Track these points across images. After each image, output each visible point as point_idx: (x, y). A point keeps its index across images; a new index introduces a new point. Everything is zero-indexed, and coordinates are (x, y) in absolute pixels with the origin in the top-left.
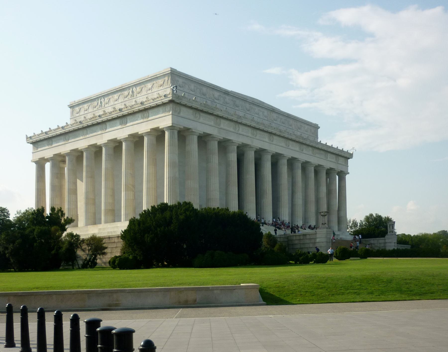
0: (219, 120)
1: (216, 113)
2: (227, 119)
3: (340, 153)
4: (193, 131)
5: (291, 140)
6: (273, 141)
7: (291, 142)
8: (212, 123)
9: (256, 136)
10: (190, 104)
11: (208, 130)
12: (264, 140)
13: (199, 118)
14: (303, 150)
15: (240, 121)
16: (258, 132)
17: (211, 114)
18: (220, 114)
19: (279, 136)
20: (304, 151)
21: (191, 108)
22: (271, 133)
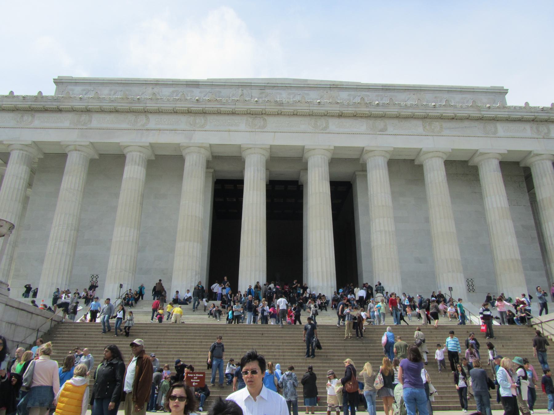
2: (102, 111)
3: (544, 116)
5: (326, 115)
12: (233, 128)
14: (384, 130)
16: (210, 118)
20: (390, 130)
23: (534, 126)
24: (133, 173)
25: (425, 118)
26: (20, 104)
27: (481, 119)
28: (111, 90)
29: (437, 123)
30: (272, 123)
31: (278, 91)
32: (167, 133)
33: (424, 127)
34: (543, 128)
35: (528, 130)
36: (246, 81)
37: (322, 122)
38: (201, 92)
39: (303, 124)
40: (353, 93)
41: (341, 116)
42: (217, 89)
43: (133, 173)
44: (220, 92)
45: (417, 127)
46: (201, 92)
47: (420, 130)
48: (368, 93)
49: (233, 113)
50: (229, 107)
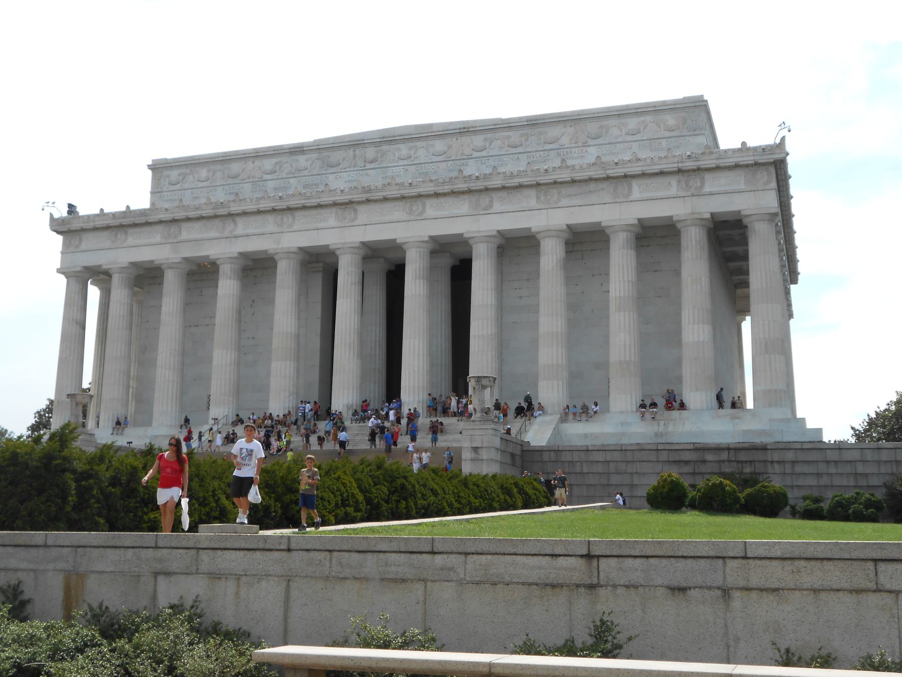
0: (174, 229)
1: (152, 219)
2: (188, 219)
4: (104, 267)
5: (420, 196)
6: (355, 219)
7: (429, 202)
8: (158, 238)
10: (91, 225)
11: (145, 255)
14: (490, 206)
15: (223, 211)
16: (298, 214)
17: (148, 224)
19: (368, 201)
20: (497, 206)
21: (95, 229)
22: (335, 204)
24: (227, 287)
25: (538, 185)
26: (111, 222)
27: (608, 178)
28: (209, 171)
29: (555, 191)
30: (364, 214)
31: (397, 146)
32: (257, 238)
34: (695, 182)
35: (673, 186)
36: (358, 138)
37: (417, 207)
39: (397, 212)
40: (489, 136)
41: (437, 195)
42: (326, 154)
43: (227, 287)
44: (329, 157)
45: (530, 199)
46: (307, 160)
49: (319, 206)
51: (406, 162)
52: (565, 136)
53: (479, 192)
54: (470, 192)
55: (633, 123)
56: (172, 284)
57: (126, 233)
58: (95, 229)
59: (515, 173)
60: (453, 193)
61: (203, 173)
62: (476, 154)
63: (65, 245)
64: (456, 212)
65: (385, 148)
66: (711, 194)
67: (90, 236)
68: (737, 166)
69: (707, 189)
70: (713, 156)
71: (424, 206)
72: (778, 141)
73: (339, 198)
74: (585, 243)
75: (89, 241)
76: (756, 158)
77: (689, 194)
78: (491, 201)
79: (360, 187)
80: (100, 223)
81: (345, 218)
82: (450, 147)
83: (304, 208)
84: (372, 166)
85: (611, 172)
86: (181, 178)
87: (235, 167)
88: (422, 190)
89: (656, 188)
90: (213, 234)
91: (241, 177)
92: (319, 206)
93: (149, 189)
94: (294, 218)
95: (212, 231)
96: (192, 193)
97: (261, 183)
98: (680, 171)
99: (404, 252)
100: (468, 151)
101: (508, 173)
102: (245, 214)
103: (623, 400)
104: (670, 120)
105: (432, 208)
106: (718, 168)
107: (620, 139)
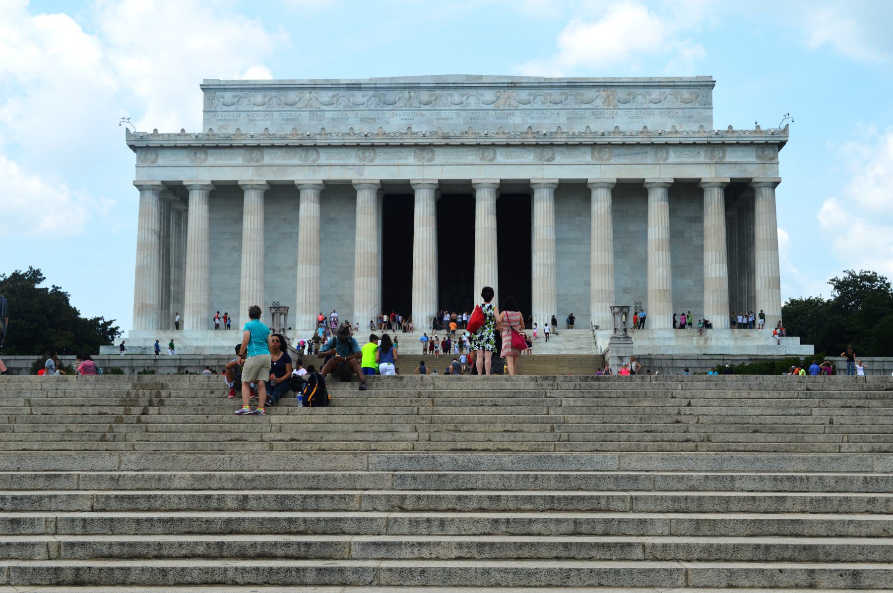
0: (256, 154)
1: (235, 143)
4: (185, 183)
6: (432, 159)
7: (499, 151)
9: (372, 161)
10: (172, 143)
11: (226, 175)
13: (205, 160)
14: (553, 159)
16: (378, 150)
17: (231, 147)
18: (254, 143)
19: (447, 145)
20: (558, 159)
22: (416, 145)
23: (710, 149)
24: (309, 209)
28: (265, 96)
30: (440, 156)
31: (450, 92)
33: (593, 155)
34: (718, 153)
35: (702, 156)
37: (489, 153)
38: (363, 96)
39: (471, 157)
40: (533, 91)
41: (508, 145)
42: (382, 92)
43: (309, 209)
45: (587, 156)
47: (588, 158)
48: (551, 91)
50: (397, 142)
51: (458, 107)
52: (599, 98)
53: (545, 146)
54: (537, 145)
55: (655, 94)
56: (253, 203)
57: (206, 154)
58: (175, 147)
59: (577, 133)
60: (523, 145)
61: (259, 98)
62: (521, 106)
63: (138, 158)
64: (522, 161)
65: (438, 92)
66: (730, 163)
67: (168, 153)
68: (752, 144)
69: (728, 159)
70: (735, 135)
71: (495, 154)
72: (783, 128)
73: (420, 141)
74: (629, 194)
75: (164, 158)
76: (767, 139)
77: (714, 161)
78: (554, 154)
79: (440, 132)
80: (180, 143)
81: (424, 158)
82: (498, 98)
83: (387, 146)
84: (427, 107)
85: (656, 140)
86: (236, 99)
87: (292, 96)
88: (496, 141)
89: (687, 156)
90: (296, 161)
91: (298, 105)
92: (401, 146)
93: (201, 108)
94: (375, 153)
95: (295, 159)
96: (248, 115)
97: (319, 113)
98: (709, 144)
99: (474, 191)
100: (514, 103)
101: (571, 133)
102: (330, 146)
103: (660, 321)
104: (686, 94)
105: (501, 156)
106: (738, 144)
107: (645, 106)
